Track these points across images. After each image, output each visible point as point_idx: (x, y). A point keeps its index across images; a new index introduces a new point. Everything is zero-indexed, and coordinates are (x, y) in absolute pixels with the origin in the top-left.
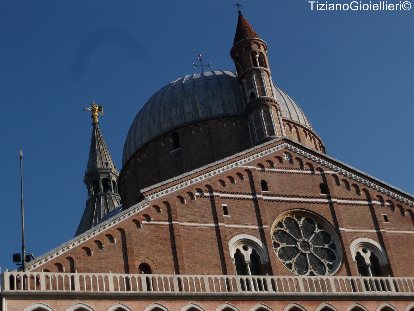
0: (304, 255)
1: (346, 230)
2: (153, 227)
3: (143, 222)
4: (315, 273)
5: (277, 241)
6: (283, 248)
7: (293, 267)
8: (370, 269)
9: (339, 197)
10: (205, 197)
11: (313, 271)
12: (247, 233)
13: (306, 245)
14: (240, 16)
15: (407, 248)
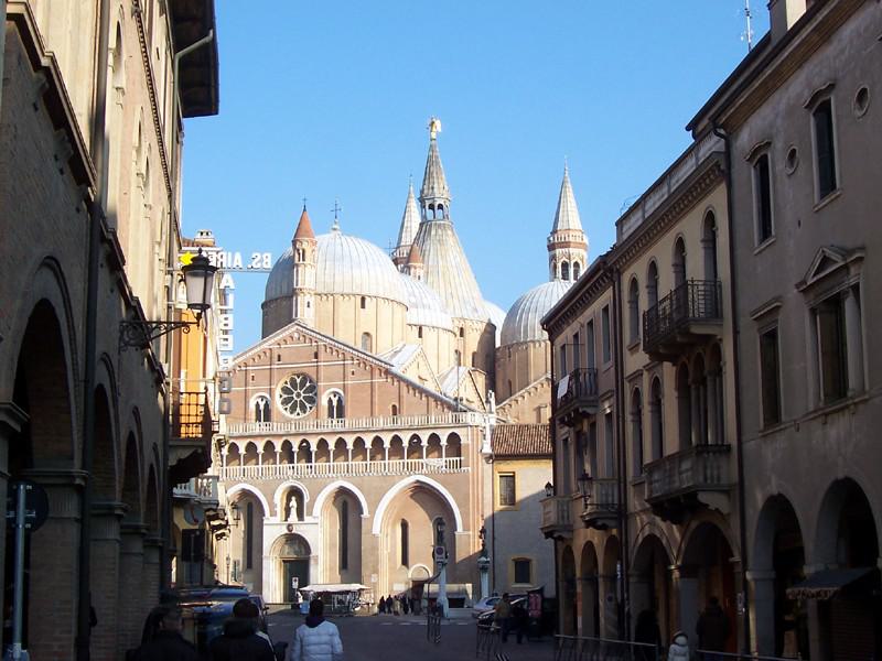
13: (298, 396)
14: (305, 210)
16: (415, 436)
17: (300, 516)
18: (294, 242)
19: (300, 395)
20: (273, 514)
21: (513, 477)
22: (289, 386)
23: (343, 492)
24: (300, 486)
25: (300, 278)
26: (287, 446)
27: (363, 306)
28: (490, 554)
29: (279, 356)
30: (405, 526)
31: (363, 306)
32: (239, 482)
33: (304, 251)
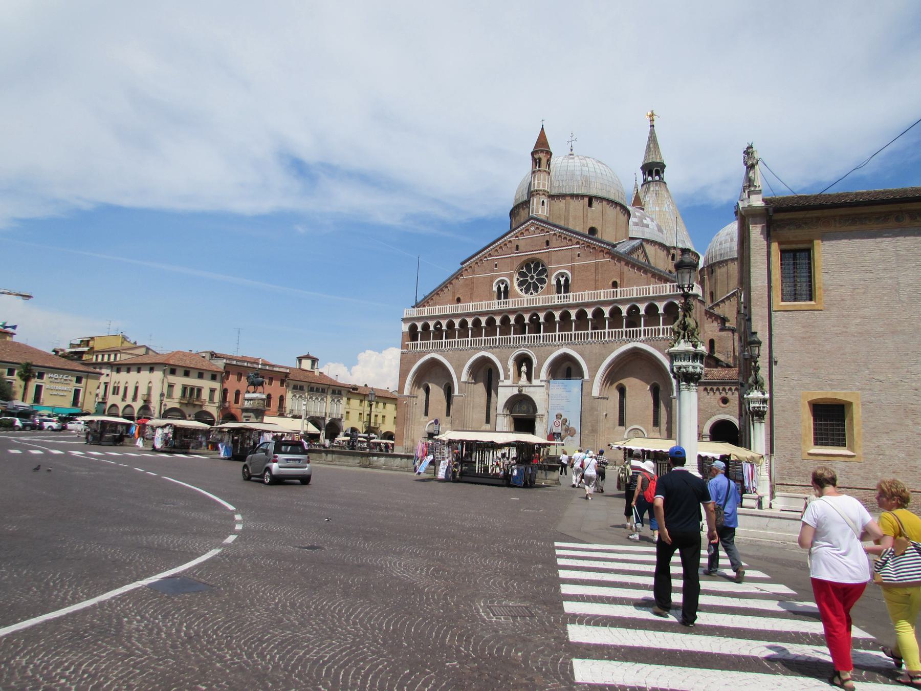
0: (530, 283)
13: (532, 278)
14: (543, 128)
17: (529, 379)
18: (533, 154)
20: (507, 377)
21: (808, 252)
22: (524, 270)
23: (566, 358)
25: (536, 182)
27: (590, 205)
28: (766, 387)
29: (517, 247)
30: (622, 391)
31: (590, 205)
32: (480, 350)
33: (540, 159)
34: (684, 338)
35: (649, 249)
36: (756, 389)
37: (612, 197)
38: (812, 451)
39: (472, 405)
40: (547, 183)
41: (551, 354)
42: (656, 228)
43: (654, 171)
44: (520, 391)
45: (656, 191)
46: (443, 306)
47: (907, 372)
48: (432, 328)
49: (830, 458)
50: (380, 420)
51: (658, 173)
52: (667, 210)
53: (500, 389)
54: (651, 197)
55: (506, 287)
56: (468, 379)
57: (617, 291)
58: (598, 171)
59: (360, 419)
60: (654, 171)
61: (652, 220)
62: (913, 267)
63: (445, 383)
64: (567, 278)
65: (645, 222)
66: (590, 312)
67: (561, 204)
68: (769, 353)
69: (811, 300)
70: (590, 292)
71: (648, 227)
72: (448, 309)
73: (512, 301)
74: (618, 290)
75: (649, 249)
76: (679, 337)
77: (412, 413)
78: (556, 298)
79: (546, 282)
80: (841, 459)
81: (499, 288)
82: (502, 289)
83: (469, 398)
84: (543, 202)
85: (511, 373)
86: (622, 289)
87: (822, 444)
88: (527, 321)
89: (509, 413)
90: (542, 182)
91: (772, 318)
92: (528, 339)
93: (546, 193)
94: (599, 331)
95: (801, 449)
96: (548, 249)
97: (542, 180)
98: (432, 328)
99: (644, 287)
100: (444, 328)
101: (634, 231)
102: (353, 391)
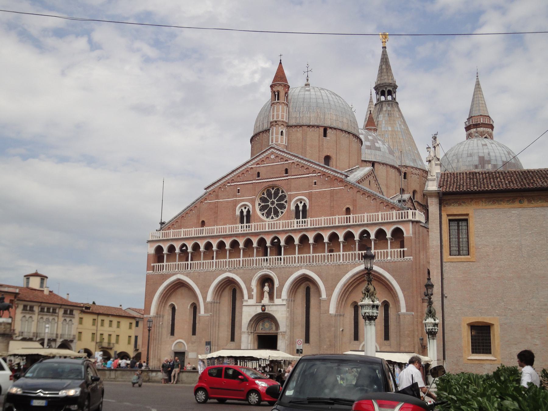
0: (271, 208)
1: (291, 193)
2: (208, 204)
3: (205, 202)
4: (274, 217)
5: (260, 203)
6: (262, 206)
7: (265, 215)
8: (301, 212)
9: (293, 175)
10: (231, 185)
11: (273, 216)
12: (246, 201)
13: (273, 203)
14: (281, 63)
15: (322, 199)
16: (365, 232)
18: (272, 86)
19: (273, 203)
21: (466, 220)
22: (265, 196)
23: (305, 279)
24: (272, 274)
25: (275, 113)
26: (262, 242)
27: (325, 135)
28: (439, 315)
29: (259, 173)
31: (325, 135)
32: (225, 271)
34: (367, 297)
35: (381, 171)
36: (430, 316)
37: (345, 128)
38: (469, 358)
39: (217, 324)
40: (285, 114)
41: (291, 274)
42: (387, 151)
43: (386, 92)
44: (264, 310)
45: (389, 111)
46: (189, 229)
47: (527, 303)
48: (177, 251)
49: (482, 362)
50: (113, 340)
51: (390, 93)
52: (399, 130)
53: (245, 309)
54: (384, 117)
55: (248, 211)
56: (214, 299)
57: (350, 217)
58: (332, 103)
59: (93, 340)
60: (386, 92)
61: (384, 143)
62: (530, 234)
63: (191, 303)
64: (304, 204)
65: (377, 145)
66: (326, 236)
67: (298, 133)
68: (442, 291)
69: (469, 255)
70: (326, 218)
71: (381, 151)
72: (193, 231)
73: (255, 225)
74: (351, 216)
75: (381, 171)
76: (365, 296)
77: (159, 332)
78: (295, 223)
79: (285, 208)
80: (488, 362)
81: (242, 212)
82: (245, 213)
83: (215, 317)
84: (282, 131)
85: (254, 293)
86: (354, 216)
87: (476, 353)
88: (268, 244)
89: (252, 331)
90: (281, 113)
91: (443, 267)
92: (270, 261)
93: (284, 124)
94: (335, 254)
95: (463, 356)
96: (287, 176)
97: (280, 111)
98: (177, 251)
99: (374, 214)
100: (190, 250)
101: (367, 155)
102: (86, 310)
